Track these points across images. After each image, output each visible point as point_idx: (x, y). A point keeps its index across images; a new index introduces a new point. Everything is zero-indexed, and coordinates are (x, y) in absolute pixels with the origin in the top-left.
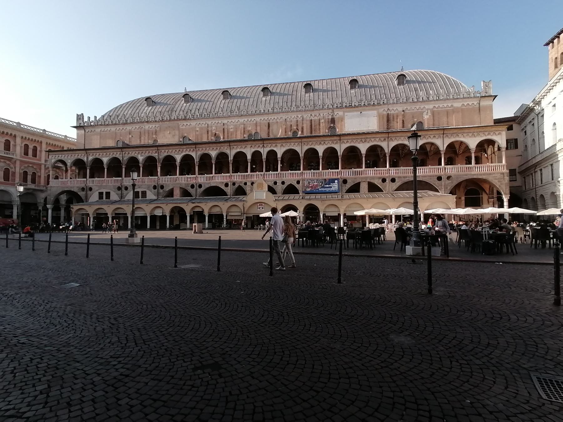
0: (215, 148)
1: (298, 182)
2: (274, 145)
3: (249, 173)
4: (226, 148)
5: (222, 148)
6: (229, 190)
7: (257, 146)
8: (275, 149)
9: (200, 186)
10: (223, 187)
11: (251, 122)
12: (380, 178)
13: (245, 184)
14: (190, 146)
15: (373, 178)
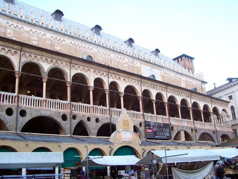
0: (49, 60)
1: (141, 124)
2: (117, 77)
3: (92, 105)
4: (64, 63)
5: (59, 62)
6: (68, 126)
7: (101, 73)
8: (118, 82)
9: (23, 113)
10: (59, 120)
11: (60, 42)
12: (190, 128)
13: (89, 119)
14: (10, 45)
15: (187, 127)
